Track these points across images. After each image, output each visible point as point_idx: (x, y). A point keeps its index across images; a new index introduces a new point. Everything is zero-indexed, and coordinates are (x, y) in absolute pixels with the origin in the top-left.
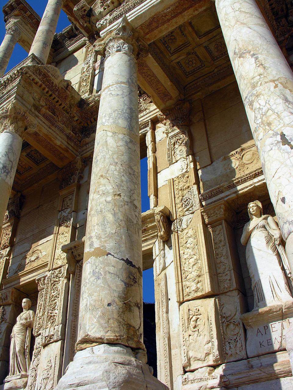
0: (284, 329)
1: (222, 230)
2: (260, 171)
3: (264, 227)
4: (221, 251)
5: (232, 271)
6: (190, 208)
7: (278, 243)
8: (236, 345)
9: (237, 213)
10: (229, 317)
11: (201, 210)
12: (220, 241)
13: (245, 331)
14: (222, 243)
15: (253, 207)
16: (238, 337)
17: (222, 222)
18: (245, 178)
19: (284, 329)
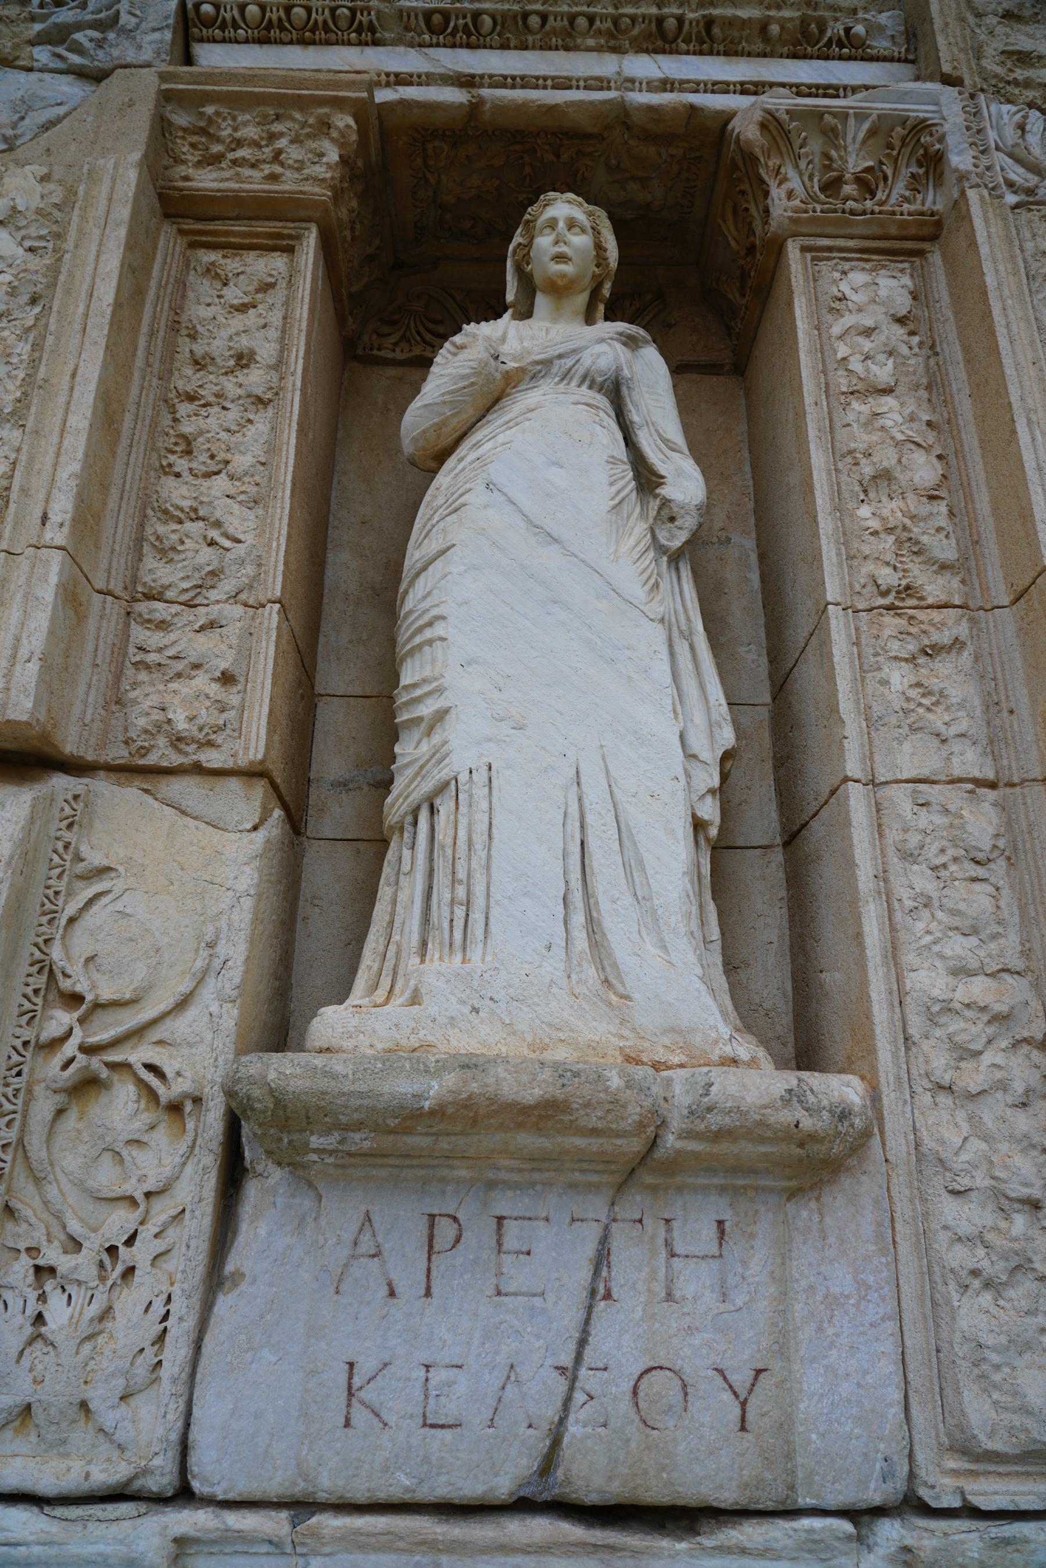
0: (608, 1296)
1: (278, 296)
2: (691, 15)
3: (615, 392)
4: (224, 435)
5: (272, 615)
6: (79, 26)
7: (676, 544)
8: (107, 1313)
11: (164, 77)
12: (240, 357)
14: (255, 379)
15: (566, 230)
16: (147, 1232)
17: (298, 238)
18: (572, 18)
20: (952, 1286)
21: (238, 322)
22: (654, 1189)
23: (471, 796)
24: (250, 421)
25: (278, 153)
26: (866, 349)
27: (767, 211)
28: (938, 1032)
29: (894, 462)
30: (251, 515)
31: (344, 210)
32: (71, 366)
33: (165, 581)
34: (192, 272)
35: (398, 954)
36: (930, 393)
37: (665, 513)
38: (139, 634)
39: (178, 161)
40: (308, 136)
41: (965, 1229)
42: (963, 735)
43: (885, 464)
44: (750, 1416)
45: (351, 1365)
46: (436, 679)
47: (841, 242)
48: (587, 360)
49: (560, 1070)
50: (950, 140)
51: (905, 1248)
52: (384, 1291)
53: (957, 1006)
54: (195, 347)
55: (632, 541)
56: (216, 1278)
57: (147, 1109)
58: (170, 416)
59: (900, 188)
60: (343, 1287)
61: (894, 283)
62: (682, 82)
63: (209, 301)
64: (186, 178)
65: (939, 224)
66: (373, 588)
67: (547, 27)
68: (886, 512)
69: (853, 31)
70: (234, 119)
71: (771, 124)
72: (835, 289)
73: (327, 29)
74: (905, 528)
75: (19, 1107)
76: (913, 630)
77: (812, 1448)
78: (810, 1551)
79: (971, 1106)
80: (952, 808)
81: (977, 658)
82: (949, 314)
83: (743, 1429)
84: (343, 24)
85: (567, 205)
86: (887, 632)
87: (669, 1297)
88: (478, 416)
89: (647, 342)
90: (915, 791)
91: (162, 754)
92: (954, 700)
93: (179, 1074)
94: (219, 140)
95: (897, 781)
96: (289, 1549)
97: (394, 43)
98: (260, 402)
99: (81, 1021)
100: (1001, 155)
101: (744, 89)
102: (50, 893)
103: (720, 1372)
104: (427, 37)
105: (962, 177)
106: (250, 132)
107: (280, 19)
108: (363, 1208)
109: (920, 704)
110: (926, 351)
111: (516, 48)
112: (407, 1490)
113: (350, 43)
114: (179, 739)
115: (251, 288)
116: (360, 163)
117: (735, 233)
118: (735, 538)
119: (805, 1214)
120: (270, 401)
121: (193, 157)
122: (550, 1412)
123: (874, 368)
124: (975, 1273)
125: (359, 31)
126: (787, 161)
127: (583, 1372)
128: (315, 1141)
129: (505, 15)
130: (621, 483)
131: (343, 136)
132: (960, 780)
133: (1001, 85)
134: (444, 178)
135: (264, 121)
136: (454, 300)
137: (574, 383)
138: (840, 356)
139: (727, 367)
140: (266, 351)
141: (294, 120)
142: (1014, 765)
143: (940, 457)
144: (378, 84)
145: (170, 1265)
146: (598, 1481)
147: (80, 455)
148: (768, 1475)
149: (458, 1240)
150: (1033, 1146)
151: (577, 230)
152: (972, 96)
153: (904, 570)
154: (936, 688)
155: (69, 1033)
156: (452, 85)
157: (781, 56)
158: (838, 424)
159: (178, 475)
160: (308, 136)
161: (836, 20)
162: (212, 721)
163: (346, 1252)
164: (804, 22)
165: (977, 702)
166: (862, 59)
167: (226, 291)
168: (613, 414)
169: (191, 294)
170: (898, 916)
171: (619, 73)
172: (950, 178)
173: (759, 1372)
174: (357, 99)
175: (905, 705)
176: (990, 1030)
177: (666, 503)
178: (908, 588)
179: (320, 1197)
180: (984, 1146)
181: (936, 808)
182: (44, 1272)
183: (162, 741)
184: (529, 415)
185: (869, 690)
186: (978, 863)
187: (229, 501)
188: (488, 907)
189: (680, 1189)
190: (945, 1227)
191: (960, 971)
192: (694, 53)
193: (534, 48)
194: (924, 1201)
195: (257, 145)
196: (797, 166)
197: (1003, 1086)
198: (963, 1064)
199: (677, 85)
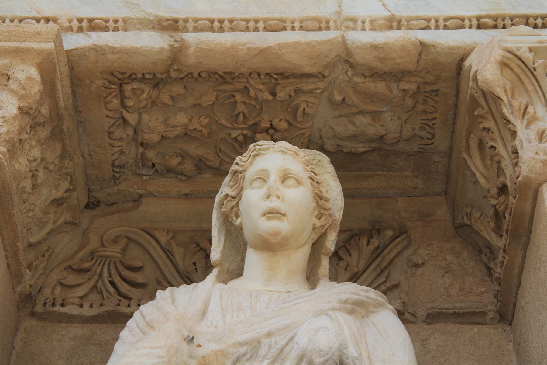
9: (92, 205)
27: (515, 152)
31: (23, 160)
48: (303, 339)
85: (279, 155)
89: (379, 305)
116: (45, 110)
117: (484, 171)
126: (535, 99)
131: (24, 88)
134: (145, 117)
136: (158, 241)
139: (490, 315)
144: (70, 29)
151: (291, 182)
171: (339, 13)
174: (41, 51)
199: (404, 22)
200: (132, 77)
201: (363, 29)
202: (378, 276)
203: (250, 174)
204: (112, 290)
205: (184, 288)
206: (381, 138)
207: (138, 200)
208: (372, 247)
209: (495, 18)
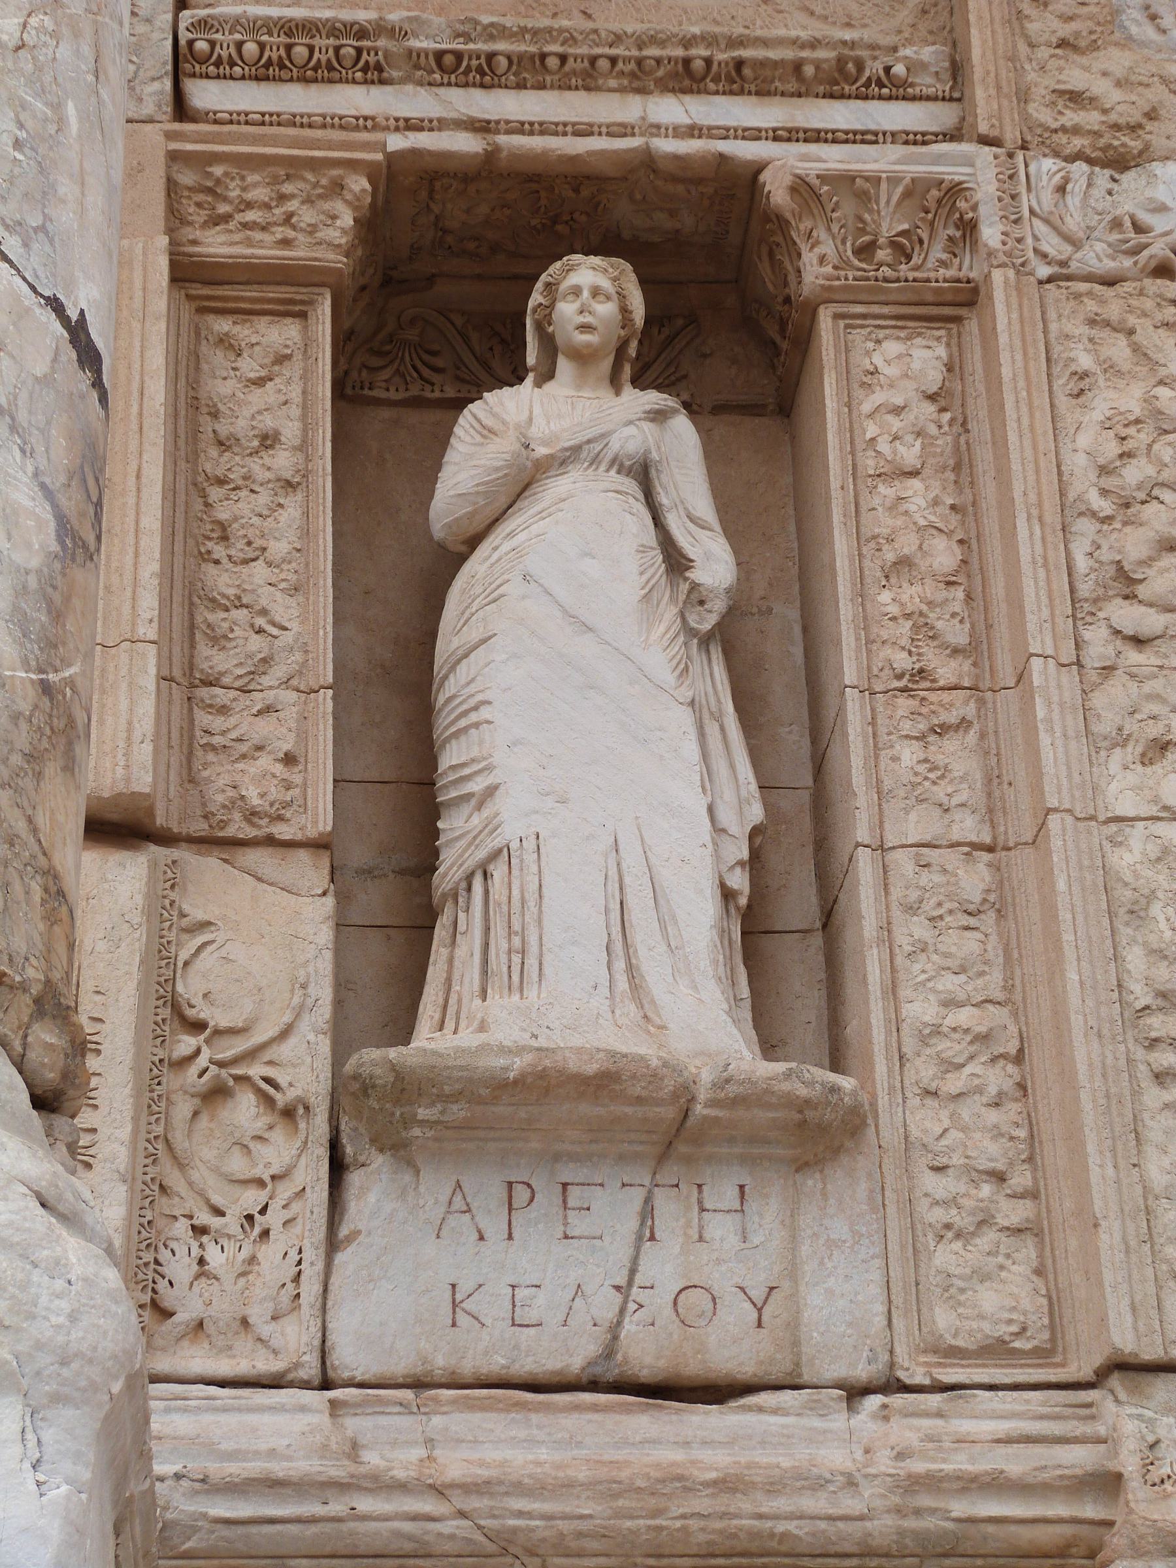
0: (652, 1238)
1: (294, 369)
3: (643, 474)
4: (255, 520)
7: (706, 626)
8: (252, 1260)
9: (387, 281)
10: (232, 1032)
12: (264, 437)
13: (338, 1167)
14: (283, 461)
15: (589, 293)
17: (311, 303)
18: (593, 60)
19: (652, 1238)
20: (930, 1236)
21: (257, 398)
22: (689, 1160)
23: (522, 861)
24: (280, 505)
25: (289, 216)
26: (895, 430)
28: (928, 1051)
29: (914, 548)
30: (292, 602)
32: (133, 467)
33: (221, 668)
34: (204, 342)
35: (459, 1001)
36: (958, 475)
37: (695, 596)
38: (203, 718)
39: (184, 222)
40: (320, 196)
41: (940, 1194)
42: (963, 805)
43: (906, 551)
44: (765, 1318)
45: (454, 1286)
46: (485, 759)
47: (876, 309)
48: (615, 445)
49: (612, 1054)
50: (982, 210)
51: (891, 1210)
52: (476, 1236)
53: (945, 1029)
54: (217, 427)
55: (662, 629)
56: (333, 1244)
57: (265, 1114)
58: (201, 500)
59: (938, 252)
60: (443, 1233)
61: (928, 353)
62: (710, 128)
63: (225, 374)
64: (194, 242)
65: (975, 291)
66: (383, 666)
67: (567, 68)
68: (905, 598)
69: (893, 70)
70: (243, 178)
71: (801, 188)
72: (867, 361)
73: (330, 68)
74: (921, 614)
75: (163, 1109)
76: (924, 710)
77: (814, 1342)
78: (811, 1409)
79: (952, 1106)
80: (949, 867)
81: (983, 736)
82: (981, 388)
83: (760, 1325)
84: (348, 63)
85: (591, 272)
86: (900, 713)
87: (701, 1239)
88: (509, 502)
89: (675, 411)
90: (917, 854)
91: (237, 828)
92: (956, 774)
93: (291, 1085)
94: (225, 199)
95: (903, 846)
96: (415, 1410)
97: (403, 81)
98: (289, 486)
99: (207, 1041)
100: (1037, 222)
101: (776, 135)
102: (164, 941)
103: (742, 1289)
104: (437, 76)
105: (991, 254)
106: (260, 194)
107: (280, 57)
108: (454, 1178)
109: (926, 778)
110: (957, 428)
111: (533, 88)
112: (503, 1367)
113: (354, 82)
114: (253, 814)
115: (267, 361)
118: (778, 608)
119: (810, 1183)
120: (299, 484)
121: (200, 217)
122: (611, 1314)
123: (902, 449)
124: (948, 1226)
125: (365, 70)
127: (635, 1290)
128: (422, 1113)
129: (521, 57)
130: (652, 571)
131: (358, 199)
132: (959, 844)
133: (1046, 135)
134: (449, 206)
135: (275, 181)
137: (603, 468)
138: (868, 436)
139: (771, 407)
140: (291, 431)
141: (305, 180)
142: (1010, 831)
143: (961, 542)
145: (297, 1229)
146: (648, 1360)
147: (157, 555)
148: (778, 1356)
149: (532, 1200)
150: (1002, 1135)
151: (602, 298)
152: (1011, 155)
153: (919, 654)
154: (941, 764)
155: (198, 1052)
156: (466, 129)
157: (817, 96)
158: (864, 508)
159: (217, 562)
160: (320, 196)
161: (875, 58)
162: (280, 797)
163: (443, 1209)
164: (841, 61)
165: (978, 776)
166: (904, 98)
167: (240, 363)
168: (641, 496)
169: (205, 367)
170: (899, 960)
171: (643, 119)
172: (983, 252)
173: (772, 1289)
175: (913, 779)
176: (972, 1049)
177: (695, 586)
178: (921, 671)
179: (418, 1172)
180: (961, 1135)
181: (935, 868)
182: (200, 1231)
183: (237, 816)
184: (561, 505)
185: (882, 766)
186: (970, 914)
187: (272, 589)
188: (541, 955)
189: (710, 1159)
190: (926, 1195)
191: (950, 1003)
192: (724, 93)
193: (552, 87)
194: (910, 1178)
195: (267, 207)
196: (829, 229)
197: (980, 1090)
198: (948, 1076)
199: (705, 131)
200: (447, 174)
201: (666, 136)
202: (668, 365)
203: (564, 286)
204: (415, 375)
205: (506, 390)
206: (677, 231)
207: (431, 279)
208: (663, 337)
209: (789, 130)
